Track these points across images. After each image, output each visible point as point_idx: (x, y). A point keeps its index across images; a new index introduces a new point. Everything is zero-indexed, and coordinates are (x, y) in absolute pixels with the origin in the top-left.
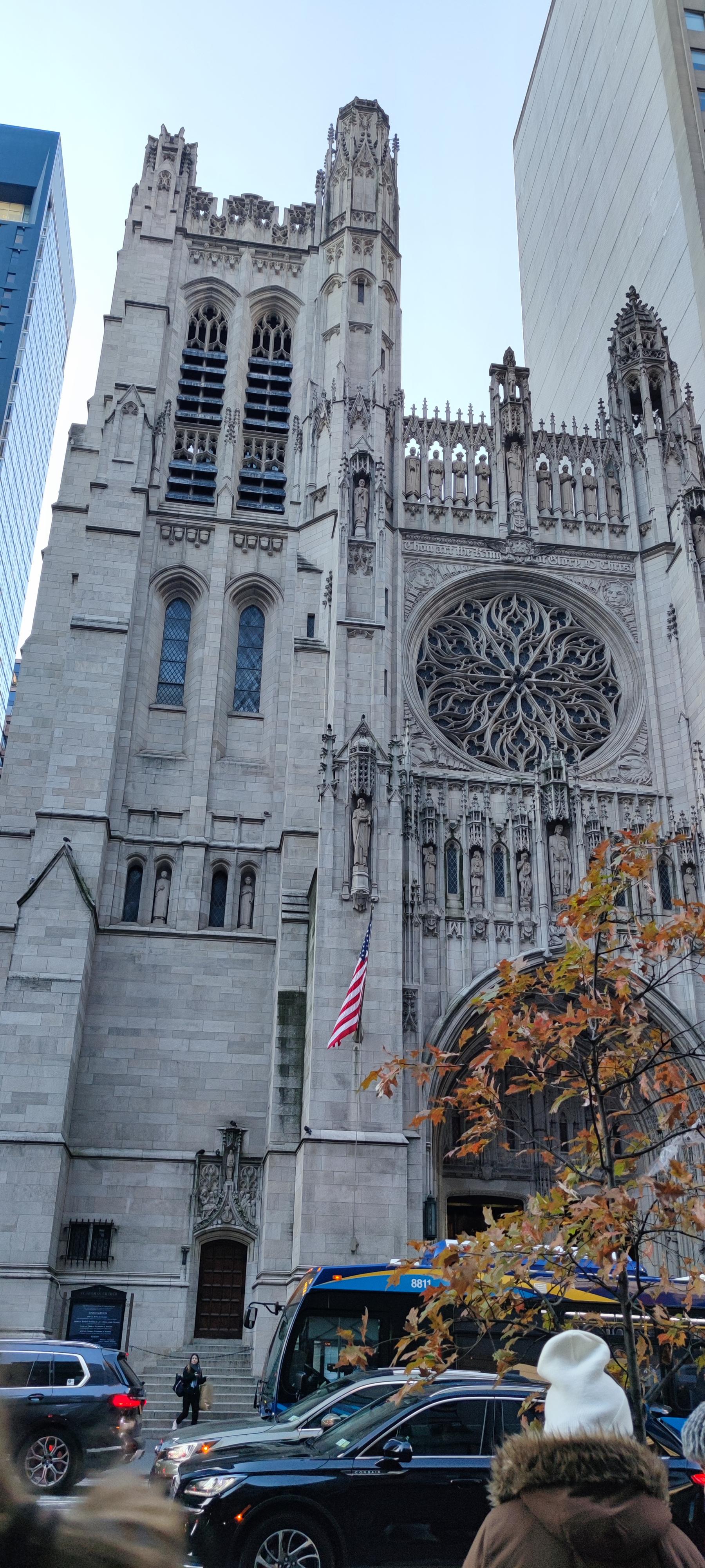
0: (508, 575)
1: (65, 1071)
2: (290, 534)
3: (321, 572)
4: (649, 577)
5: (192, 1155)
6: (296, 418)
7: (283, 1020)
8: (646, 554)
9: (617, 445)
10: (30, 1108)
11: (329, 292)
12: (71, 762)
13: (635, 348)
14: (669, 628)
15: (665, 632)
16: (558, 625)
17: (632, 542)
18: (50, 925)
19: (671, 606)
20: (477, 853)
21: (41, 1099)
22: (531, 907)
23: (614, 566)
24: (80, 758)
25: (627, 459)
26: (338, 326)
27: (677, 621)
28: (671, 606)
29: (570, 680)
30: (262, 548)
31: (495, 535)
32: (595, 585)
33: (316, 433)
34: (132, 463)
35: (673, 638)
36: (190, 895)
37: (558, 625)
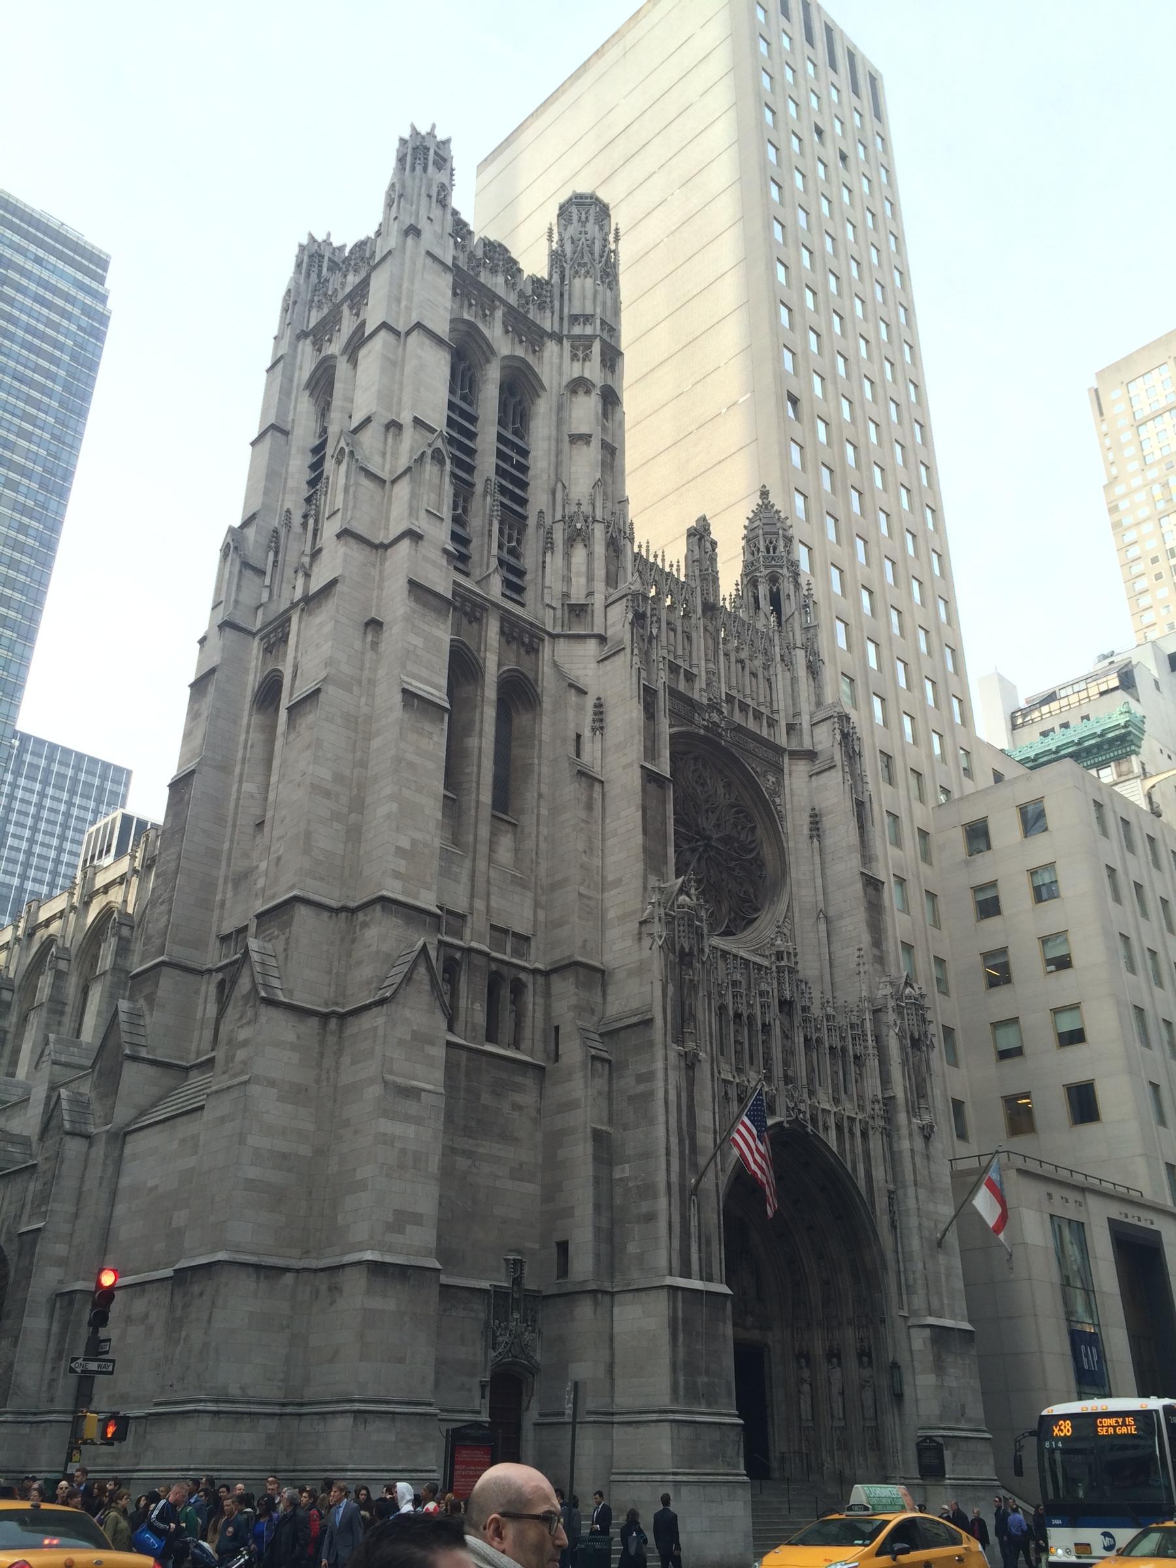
0: (704, 739)
2: (547, 638)
3: (585, 693)
4: (794, 775)
5: (485, 1284)
6: (541, 512)
7: (597, 1159)
8: (794, 755)
9: (771, 640)
10: (409, 1229)
11: (574, 392)
12: (405, 843)
13: (775, 549)
14: (811, 830)
15: (806, 831)
16: (727, 796)
17: (782, 739)
19: (813, 809)
20: (737, 1020)
21: (417, 1219)
23: (770, 754)
24: (414, 842)
25: (778, 658)
26: (590, 436)
28: (813, 809)
29: (736, 852)
30: (523, 644)
31: (696, 696)
32: (758, 769)
33: (570, 542)
34: (442, 519)
35: (815, 840)
36: (477, 1006)
37: (727, 796)
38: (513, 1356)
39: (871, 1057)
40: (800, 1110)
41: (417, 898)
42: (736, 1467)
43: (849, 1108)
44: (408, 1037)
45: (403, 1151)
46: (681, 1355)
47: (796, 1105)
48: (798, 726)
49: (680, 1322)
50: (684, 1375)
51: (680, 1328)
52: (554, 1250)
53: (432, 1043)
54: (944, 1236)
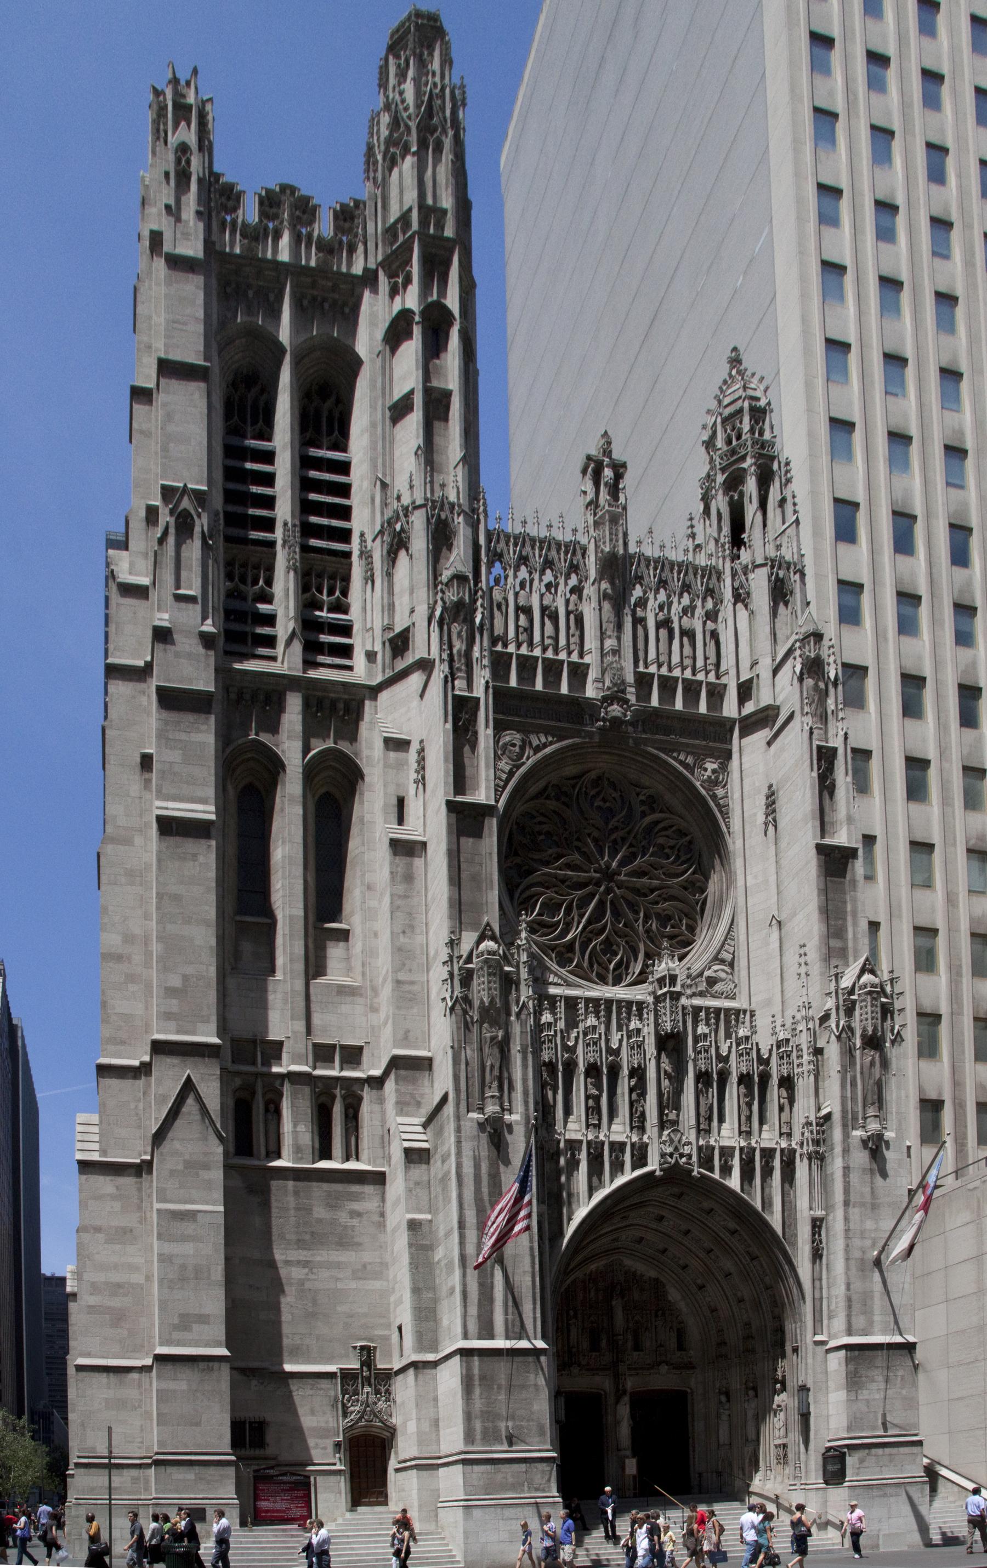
1: (220, 1293)
10: (195, 1327)
18: (187, 1157)
19: (770, 786)
21: (203, 1319)
22: (642, 1129)
24: (185, 978)
27: (777, 805)
38: (366, 1421)
39: (806, 1074)
40: (682, 1156)
41: (194, 1033)
42: (550, 1491)
43: (768, 1138)
44: (180, 1167)
45: (183, 1267)
46: (478, 1404)
47: (676, 1149)
48: (755, 681)
49: (477, 1378)
50: (483, 1422)
51: (477, 1383)
52: (397, 1330)
53: (206, 1167)
54: (881, 1253)
